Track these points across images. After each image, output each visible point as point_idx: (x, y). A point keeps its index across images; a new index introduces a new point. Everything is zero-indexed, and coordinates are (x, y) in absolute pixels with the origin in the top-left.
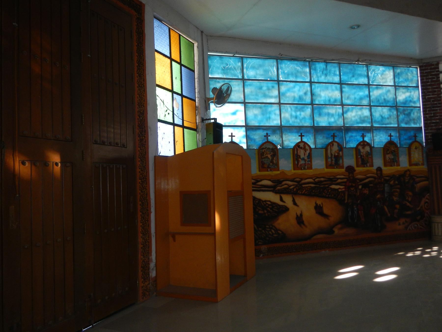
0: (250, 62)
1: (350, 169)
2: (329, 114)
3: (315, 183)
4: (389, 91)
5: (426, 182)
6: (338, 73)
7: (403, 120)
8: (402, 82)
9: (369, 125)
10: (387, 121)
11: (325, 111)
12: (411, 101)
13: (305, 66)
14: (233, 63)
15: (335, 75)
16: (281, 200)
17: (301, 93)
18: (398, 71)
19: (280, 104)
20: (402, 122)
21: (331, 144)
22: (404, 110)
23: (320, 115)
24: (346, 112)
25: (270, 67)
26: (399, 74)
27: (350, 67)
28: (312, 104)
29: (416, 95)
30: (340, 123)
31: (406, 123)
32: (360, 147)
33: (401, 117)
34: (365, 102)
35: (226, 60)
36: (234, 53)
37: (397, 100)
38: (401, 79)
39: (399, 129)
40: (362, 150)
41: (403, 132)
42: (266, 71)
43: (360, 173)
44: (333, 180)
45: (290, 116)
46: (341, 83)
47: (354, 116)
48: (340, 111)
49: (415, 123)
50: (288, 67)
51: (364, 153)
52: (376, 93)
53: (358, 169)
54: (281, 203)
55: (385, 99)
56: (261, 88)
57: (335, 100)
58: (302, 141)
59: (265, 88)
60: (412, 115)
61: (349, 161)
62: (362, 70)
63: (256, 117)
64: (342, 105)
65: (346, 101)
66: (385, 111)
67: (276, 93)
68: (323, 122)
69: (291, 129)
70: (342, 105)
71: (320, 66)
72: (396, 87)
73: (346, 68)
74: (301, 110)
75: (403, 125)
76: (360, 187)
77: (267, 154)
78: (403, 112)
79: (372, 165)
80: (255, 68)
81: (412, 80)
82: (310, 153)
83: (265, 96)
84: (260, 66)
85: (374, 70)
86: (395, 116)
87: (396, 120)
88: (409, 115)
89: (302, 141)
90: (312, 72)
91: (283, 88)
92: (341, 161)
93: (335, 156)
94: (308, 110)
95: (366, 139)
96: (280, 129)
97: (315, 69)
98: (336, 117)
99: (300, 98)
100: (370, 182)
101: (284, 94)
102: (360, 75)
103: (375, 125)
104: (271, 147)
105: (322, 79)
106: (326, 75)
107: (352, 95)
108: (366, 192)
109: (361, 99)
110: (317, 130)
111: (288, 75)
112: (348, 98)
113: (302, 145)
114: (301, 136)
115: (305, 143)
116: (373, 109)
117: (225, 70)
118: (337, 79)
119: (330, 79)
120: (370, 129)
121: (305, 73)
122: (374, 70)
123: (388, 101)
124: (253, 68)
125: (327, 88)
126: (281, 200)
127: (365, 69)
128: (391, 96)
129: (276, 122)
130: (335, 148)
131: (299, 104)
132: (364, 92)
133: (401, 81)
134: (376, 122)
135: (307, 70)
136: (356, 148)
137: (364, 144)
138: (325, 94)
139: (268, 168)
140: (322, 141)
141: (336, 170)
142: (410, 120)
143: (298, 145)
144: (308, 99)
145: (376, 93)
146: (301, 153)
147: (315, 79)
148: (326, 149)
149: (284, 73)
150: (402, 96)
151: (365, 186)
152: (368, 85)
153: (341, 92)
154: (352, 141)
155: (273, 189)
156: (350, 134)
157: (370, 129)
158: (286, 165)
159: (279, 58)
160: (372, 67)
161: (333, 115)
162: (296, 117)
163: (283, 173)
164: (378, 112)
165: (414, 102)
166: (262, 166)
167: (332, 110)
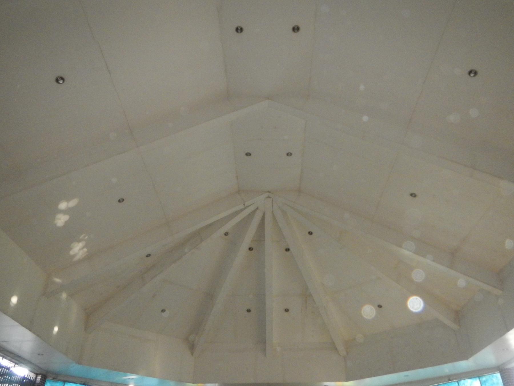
18: (484, 379)
26: (485, 381)
85: (464, 384)
122: (464, 384)
127: (457, 384)
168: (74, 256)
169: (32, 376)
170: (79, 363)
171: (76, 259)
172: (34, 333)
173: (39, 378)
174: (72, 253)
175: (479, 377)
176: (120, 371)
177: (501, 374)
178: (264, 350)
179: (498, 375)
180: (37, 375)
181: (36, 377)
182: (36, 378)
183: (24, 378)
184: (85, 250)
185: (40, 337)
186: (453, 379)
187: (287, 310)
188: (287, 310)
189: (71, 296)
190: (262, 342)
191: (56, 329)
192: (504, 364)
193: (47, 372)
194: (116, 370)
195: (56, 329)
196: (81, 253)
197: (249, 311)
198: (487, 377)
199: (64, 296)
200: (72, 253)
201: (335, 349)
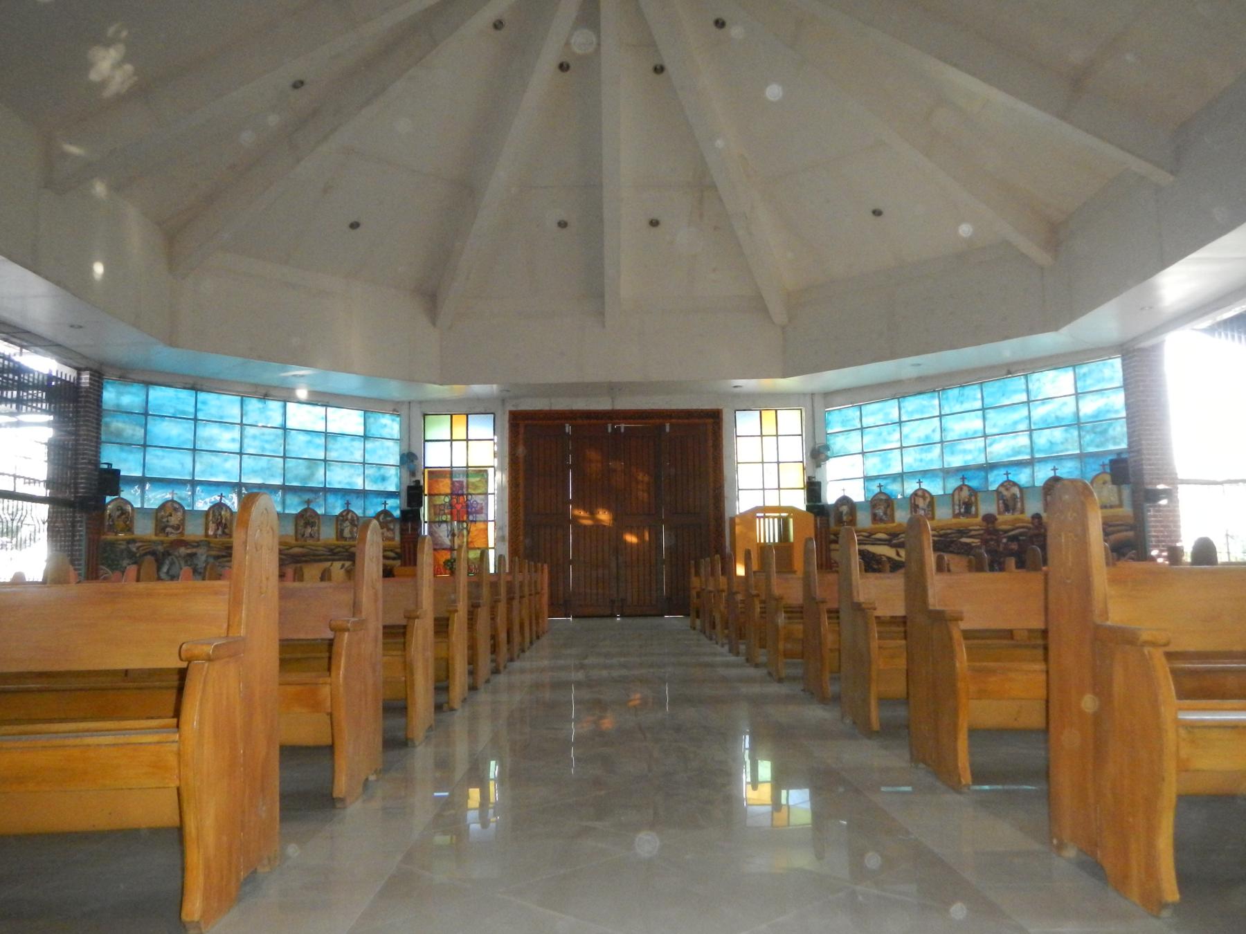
0: (868, 409)
1: (989, 518)
2: (965, 451)
3: (941, 536)
4: (1065, 404)
5: (1131, 534)
6: (979, 396)
7: (1092, 441)
8: (1091, 385)
9: (1028, 457)
10: (1061, 447)
11: (961, 447)
12: (1108, 411)
13: (933, 398)
14: (853, 413)
15: (975, 399)
16: (898, 554)
17: (929, 431)
18: (1084, 369)
19: (902, 448)
20: (1088, 445)
21: (960, 488)
22: (1094, 427)
23: (953, 453)
24: (991, 445)
25: (891, 409)
26: (1085, 375)
27: (997, 384)
28: (942, 442)
29: (1117, 401)
30: (981, 460)
31: (1097, 446)
32: (1002, 489)
33: (1088, 438)
34: (1023, 426)
35: (844, 411)
36: (852, 403)
37: (1081, 414)
38: (1089, 381)
39: (1082, 457)
40: (1005, 493)
41: (1091, 460)
42: (887, 414)
43: (1005, 523)
44: (963, 532)
45: (912, 460)
46: (983, 409)
47: (1001, 449)
48: (982, 444)
49: (1115, 444)
50: (912, 404)
51: (1010, 498)
52: (1039, 412)
53: (1000, 518)
54: (897, 558)
55: (1057, 417)
56: (880, 434)
57: (975, 432)
58: (920, 489)
59: (885, 434)
60: (1111, 432)
61: (987, 507)
62: (1019, 382)
63: (875, 466)
64: (985, 436)
65: (988, 431)
66: (1058, 434)
67: (897, 436)
68: (956, 461)
69: (913, 474)
70: (985, 436)
71: (954, 392)
72: (1077, 395)
73: (992, 388)
74: (928, 451)
75: (1091, 449)
76: (1004, 540)
77: (882, 504)
78: (1093, 430)
79: (1022, 512)
80: (878, 412)
81: (1111, 379)
82: (932, 501)
83: (885, 441)
84: (881, 410)
86: (1076, 438)
87: (1077, 444)
88: (1105, 431)
89: (920, 489)
90: (943, 402)
91: (906, 429)
92: (973, 509)
93: (965, 503)
94: (938, 448)
95: (1011, 477)
96: (901, 477)
97: (947, 399)
98: (976, 454)
99: (927, 437)
100: (1021, 534)
101: (907, 436)
102: (1015, 392)
103: (1037, 456)
104: (883, 497)
105: (958, 408)
106: (962, 403)
107: (998, 421)
108: (1014, 546)
109: (1016, 423)
110: (947, 473)
111: (912, 413)
112: (994, 426)
113: (920, 493)
114: (920, 482)
115: (924, 491)
116: (1035, 434)
117: (843, 422)
118: (978, 405)
119: (967, 406)
120: (1031, 463)
121: (933, 407)
123: (1063, 419)
124: (873, 413)
125: (963, 419)
126: (898, 554)
127: (1023, 380)
128: (1068, 409)
129: (896, 469)
130: (965, 493)
131: (927, 444)
132: (1024, 412)
133: (1090, 384)
134: (1040, 451)
135: (936, 402)
136: (997, 491)
137: (1009, 484)
138: (957, 427)
139: (881, 520)
140: (953, 484)
141: (963, 520)
142: (1107, 440)
143: (915, 494)
144: (937, 438)
145: (1039, 412)
146: (921, 503)
147: (946, 410)
148: (953, 495)
149: (907, 412)
150: (1089, 407)
151: (1014, 539)
152: (1028, 402)
153: (984, 419)
154: (996, 480)
155: (888, 543)
156: (995, 472)
157: (1031, 463)
158: (902, 516)
159: (900, 396)
160: (1036, 376)
161: (970, 451)
162: (921, 460)
163: (900, 525)
164: (1042, 439)
165: (1117, 412)
166: (875, 518)
167: (969, 445)
168: (103, 84)
169: (68, 373)
170: (172, 344)
171: (109, 92)
172: (46, 278)
173: (85, 378)
174: (94, 76)
175: (1074, 367)
176: (270, 360)
177: (1123, 360)
178: (601, 313)
179: (1117, 362)
180: (79, 370)
181: (79, 374)
182: (79, 378)
183: (50, 378)
184: (129, 68)
185: (65, 287)
186: (1016, 371)
187: (654, 223)
188: (654, 223)
189: (117, 188)
190: (594, 292)
191: (99, 269)
192: (1134, 339)
193: (102, 364)
194: (260, 358)
195: (99, 269)
196: (119, 76)
197: (563, 225)
198: (1093, 366)
199: (100, 189)
200: (94, 76)
201: (765, 310)
